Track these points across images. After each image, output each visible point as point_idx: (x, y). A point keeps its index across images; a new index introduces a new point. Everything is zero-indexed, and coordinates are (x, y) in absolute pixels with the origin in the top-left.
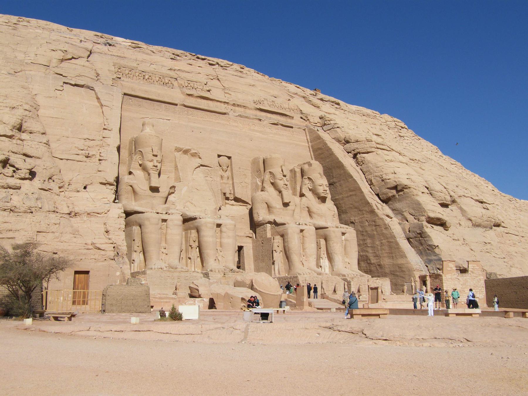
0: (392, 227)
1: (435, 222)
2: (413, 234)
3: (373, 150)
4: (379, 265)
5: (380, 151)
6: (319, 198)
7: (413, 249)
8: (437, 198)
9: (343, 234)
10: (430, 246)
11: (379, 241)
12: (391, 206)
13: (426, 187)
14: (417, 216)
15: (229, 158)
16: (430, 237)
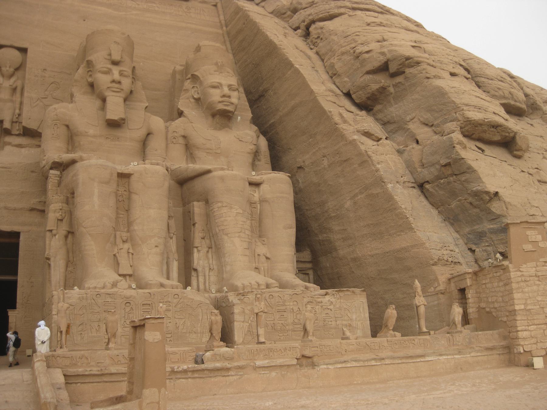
0: (375, 158)
1: (487, 136)
2: (432, 169)
3: (342, 10)
4: (355, 260)
5: (359, 13)
6: (213, 116)
7: (434, 212)
8: (493, 92)
9: (255, 185)
10: (477, 194)
11: (351, 199)
12: (380, 116)
13: (461, 65)
14: (438, 125)
15: (23, 51)
16: (474, 171)
